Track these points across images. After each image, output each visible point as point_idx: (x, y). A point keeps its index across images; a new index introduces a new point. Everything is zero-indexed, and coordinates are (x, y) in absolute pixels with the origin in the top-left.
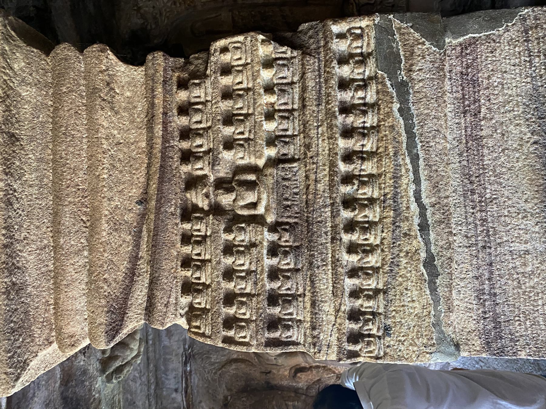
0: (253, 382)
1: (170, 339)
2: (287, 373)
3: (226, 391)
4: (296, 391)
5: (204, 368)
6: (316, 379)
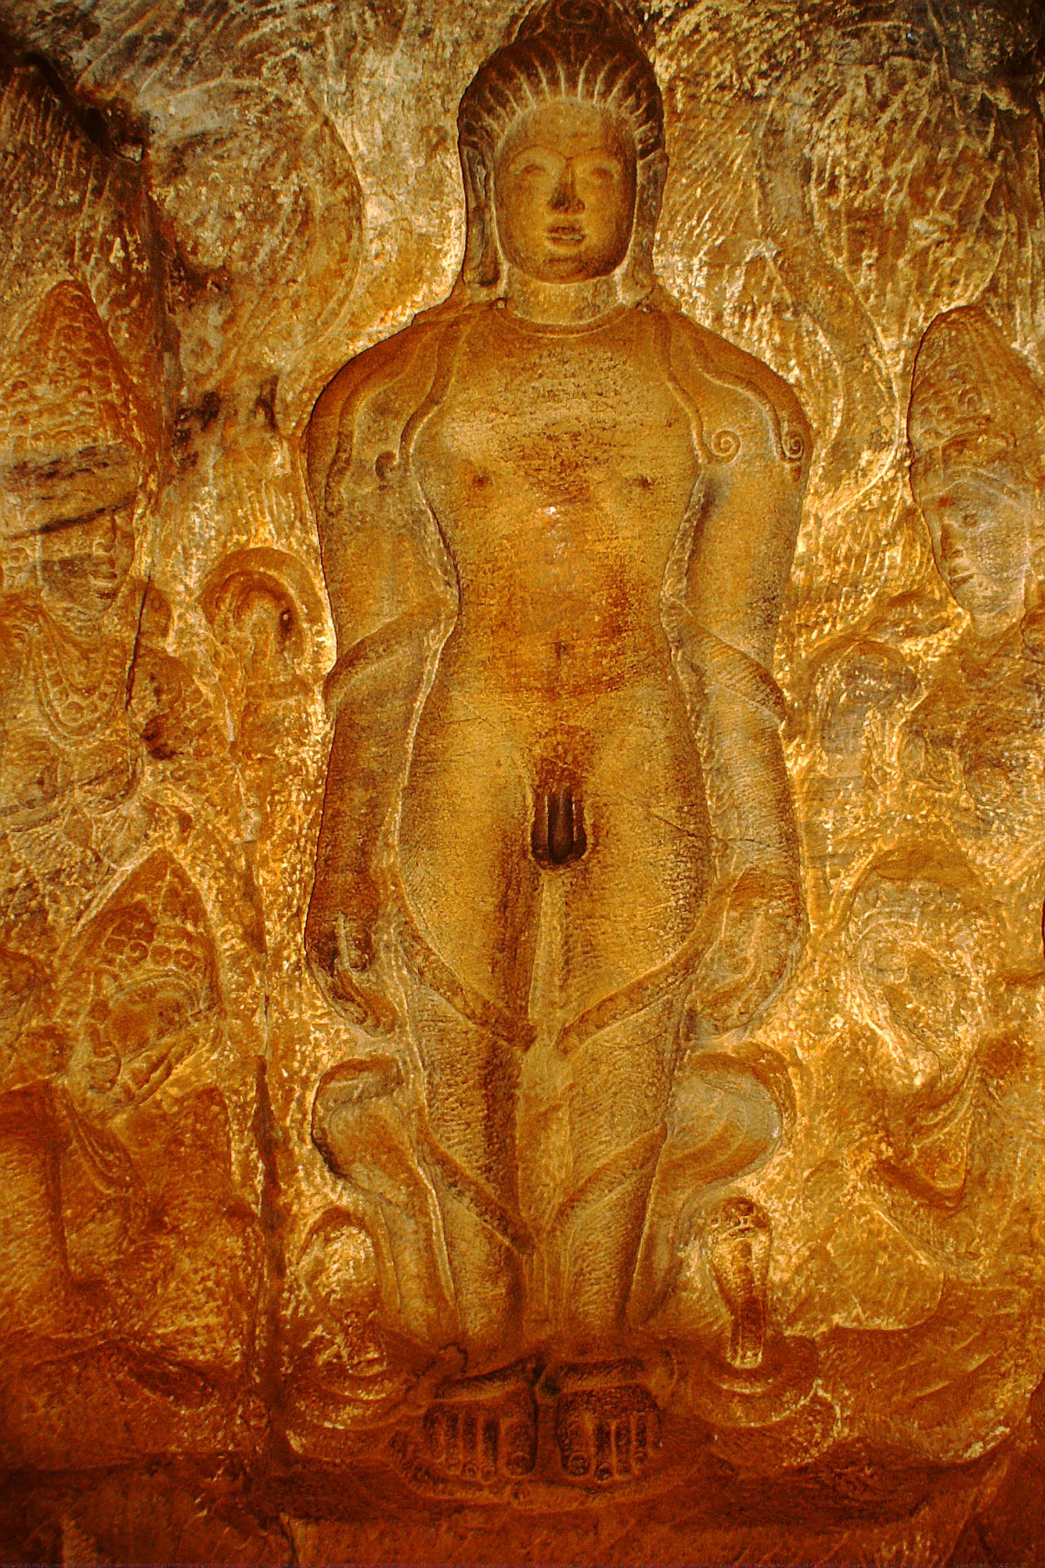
2: (265, 535)
3: (175, 133)
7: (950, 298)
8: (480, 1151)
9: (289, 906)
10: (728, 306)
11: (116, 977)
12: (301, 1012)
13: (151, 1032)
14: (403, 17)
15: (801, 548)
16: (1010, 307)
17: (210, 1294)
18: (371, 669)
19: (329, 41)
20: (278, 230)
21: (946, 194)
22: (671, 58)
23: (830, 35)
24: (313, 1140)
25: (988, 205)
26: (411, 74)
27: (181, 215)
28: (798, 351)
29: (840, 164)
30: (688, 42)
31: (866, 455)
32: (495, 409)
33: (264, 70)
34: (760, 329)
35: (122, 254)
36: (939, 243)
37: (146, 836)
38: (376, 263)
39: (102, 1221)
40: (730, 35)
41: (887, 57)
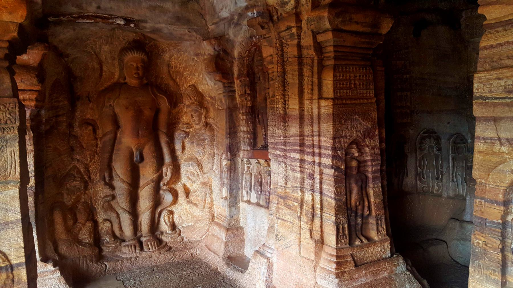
0: (79, 83)
1: (147, 8)
2: (89, 117)
3: (73, 56)
4: (70, 126)
5: (100, 38)
6: (83, 144)
18: (109, 136)
23: (171, 48)
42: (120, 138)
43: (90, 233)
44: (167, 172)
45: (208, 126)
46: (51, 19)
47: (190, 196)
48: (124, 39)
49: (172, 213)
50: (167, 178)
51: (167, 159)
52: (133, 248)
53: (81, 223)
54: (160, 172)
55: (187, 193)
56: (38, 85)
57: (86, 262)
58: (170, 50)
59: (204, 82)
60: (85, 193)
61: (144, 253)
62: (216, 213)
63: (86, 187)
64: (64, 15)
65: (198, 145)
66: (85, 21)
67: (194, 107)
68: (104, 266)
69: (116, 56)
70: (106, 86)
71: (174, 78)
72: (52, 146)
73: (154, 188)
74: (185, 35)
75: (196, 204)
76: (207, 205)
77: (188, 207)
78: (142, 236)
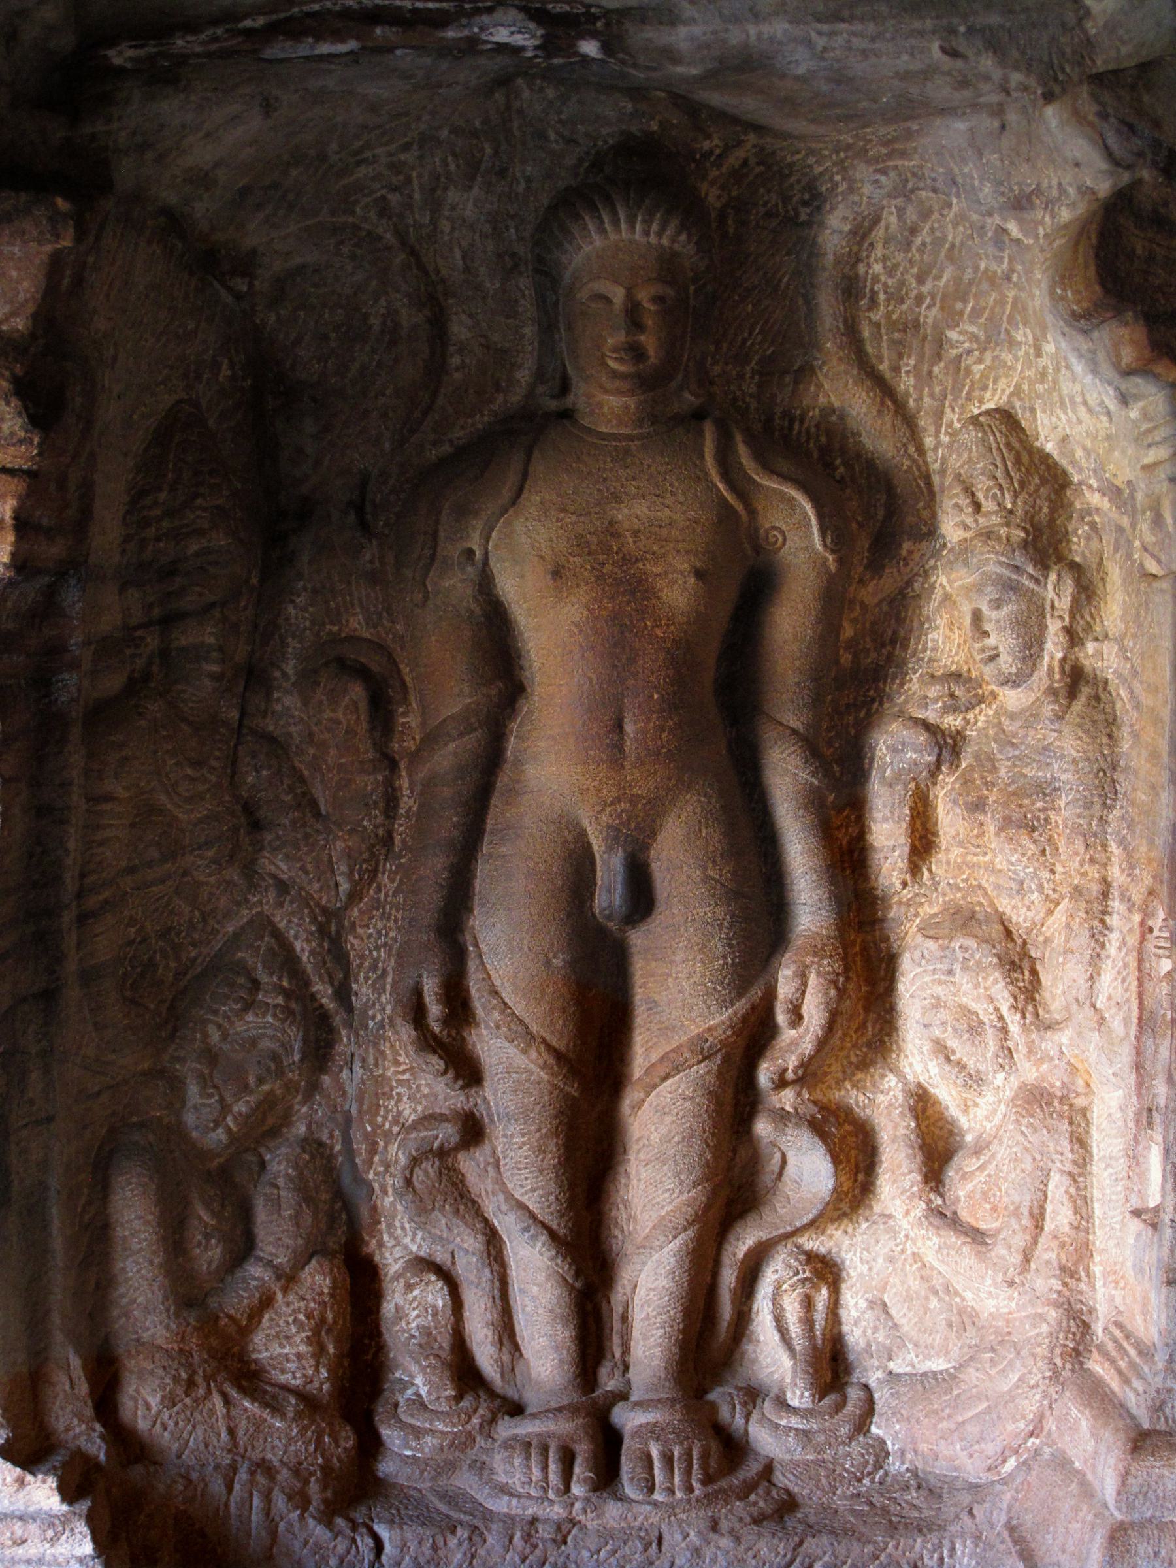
2: (356, 623)
4: (254, 678)
7: (981, 402)
8: (552, 1198)
9: (374, 968)
10: (778, 410)
11: (219, 1026)
12: (385, 1069)
13: (252, 1080)
14: (480, 161)
15: (848, 632)
16: (1032, 410)
17: (301, 1326)
18: (452, 746)
19: (415, 182)
20: (368, 348)
21: (973, 309)
22: (722, 188)
23: (862, 171)
24: (395, 1190)
25: (1011, 319)
26: (488, 206)
27: (281, 336)
28: (843, 450)
29: (879, 281)
30: (737, 175)
31: (906, 546)
32: (564, 510)
33: (358, 210)
34: (808, 431)
35: (229, 373)
36: (969, 352)
37: (247, 901)
38: (457, 375)
39: (206, 1249)
40: (775, 168)
41: (912, 191)
42: (518, 762)
43: (316, 1332)
44: (805, 996)
45: (1085, 691)
46: (121, 56)
47: (951, 1173)
48: (571, 141)
49: (826, 1271)
50: (796, 1042)
51: (810, 908)
52: (553, 1467)
53: (269, 1264)
54: (756, 992)
55: (937, 1151)
56: (21, 442)
57: (267, 1498)
58: (851, 190)
59: (1066, 387)
60: (314, 1087)
61: (613, 1511)
62: (1102, 1309)
63: (320, 1050)
64: (191, 27)
65: (1006, 823)
66: (305, 48)
67: (991, 562)
68: (365, 1544)
69: (521, 250)
70: (458, 434)
71: (884, 367)
72: (121, 793)
73: (715, 1096)
74: (927, 74)
75: (977, 1236)
76: (1048, 1253)
77: (931, 1244)
78: (622, 1396)
